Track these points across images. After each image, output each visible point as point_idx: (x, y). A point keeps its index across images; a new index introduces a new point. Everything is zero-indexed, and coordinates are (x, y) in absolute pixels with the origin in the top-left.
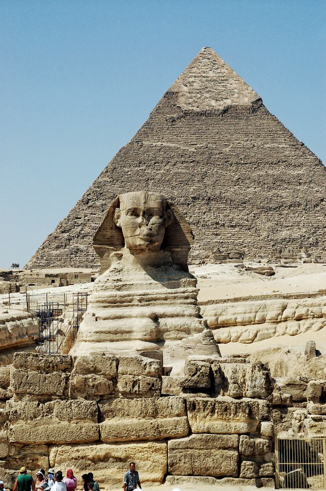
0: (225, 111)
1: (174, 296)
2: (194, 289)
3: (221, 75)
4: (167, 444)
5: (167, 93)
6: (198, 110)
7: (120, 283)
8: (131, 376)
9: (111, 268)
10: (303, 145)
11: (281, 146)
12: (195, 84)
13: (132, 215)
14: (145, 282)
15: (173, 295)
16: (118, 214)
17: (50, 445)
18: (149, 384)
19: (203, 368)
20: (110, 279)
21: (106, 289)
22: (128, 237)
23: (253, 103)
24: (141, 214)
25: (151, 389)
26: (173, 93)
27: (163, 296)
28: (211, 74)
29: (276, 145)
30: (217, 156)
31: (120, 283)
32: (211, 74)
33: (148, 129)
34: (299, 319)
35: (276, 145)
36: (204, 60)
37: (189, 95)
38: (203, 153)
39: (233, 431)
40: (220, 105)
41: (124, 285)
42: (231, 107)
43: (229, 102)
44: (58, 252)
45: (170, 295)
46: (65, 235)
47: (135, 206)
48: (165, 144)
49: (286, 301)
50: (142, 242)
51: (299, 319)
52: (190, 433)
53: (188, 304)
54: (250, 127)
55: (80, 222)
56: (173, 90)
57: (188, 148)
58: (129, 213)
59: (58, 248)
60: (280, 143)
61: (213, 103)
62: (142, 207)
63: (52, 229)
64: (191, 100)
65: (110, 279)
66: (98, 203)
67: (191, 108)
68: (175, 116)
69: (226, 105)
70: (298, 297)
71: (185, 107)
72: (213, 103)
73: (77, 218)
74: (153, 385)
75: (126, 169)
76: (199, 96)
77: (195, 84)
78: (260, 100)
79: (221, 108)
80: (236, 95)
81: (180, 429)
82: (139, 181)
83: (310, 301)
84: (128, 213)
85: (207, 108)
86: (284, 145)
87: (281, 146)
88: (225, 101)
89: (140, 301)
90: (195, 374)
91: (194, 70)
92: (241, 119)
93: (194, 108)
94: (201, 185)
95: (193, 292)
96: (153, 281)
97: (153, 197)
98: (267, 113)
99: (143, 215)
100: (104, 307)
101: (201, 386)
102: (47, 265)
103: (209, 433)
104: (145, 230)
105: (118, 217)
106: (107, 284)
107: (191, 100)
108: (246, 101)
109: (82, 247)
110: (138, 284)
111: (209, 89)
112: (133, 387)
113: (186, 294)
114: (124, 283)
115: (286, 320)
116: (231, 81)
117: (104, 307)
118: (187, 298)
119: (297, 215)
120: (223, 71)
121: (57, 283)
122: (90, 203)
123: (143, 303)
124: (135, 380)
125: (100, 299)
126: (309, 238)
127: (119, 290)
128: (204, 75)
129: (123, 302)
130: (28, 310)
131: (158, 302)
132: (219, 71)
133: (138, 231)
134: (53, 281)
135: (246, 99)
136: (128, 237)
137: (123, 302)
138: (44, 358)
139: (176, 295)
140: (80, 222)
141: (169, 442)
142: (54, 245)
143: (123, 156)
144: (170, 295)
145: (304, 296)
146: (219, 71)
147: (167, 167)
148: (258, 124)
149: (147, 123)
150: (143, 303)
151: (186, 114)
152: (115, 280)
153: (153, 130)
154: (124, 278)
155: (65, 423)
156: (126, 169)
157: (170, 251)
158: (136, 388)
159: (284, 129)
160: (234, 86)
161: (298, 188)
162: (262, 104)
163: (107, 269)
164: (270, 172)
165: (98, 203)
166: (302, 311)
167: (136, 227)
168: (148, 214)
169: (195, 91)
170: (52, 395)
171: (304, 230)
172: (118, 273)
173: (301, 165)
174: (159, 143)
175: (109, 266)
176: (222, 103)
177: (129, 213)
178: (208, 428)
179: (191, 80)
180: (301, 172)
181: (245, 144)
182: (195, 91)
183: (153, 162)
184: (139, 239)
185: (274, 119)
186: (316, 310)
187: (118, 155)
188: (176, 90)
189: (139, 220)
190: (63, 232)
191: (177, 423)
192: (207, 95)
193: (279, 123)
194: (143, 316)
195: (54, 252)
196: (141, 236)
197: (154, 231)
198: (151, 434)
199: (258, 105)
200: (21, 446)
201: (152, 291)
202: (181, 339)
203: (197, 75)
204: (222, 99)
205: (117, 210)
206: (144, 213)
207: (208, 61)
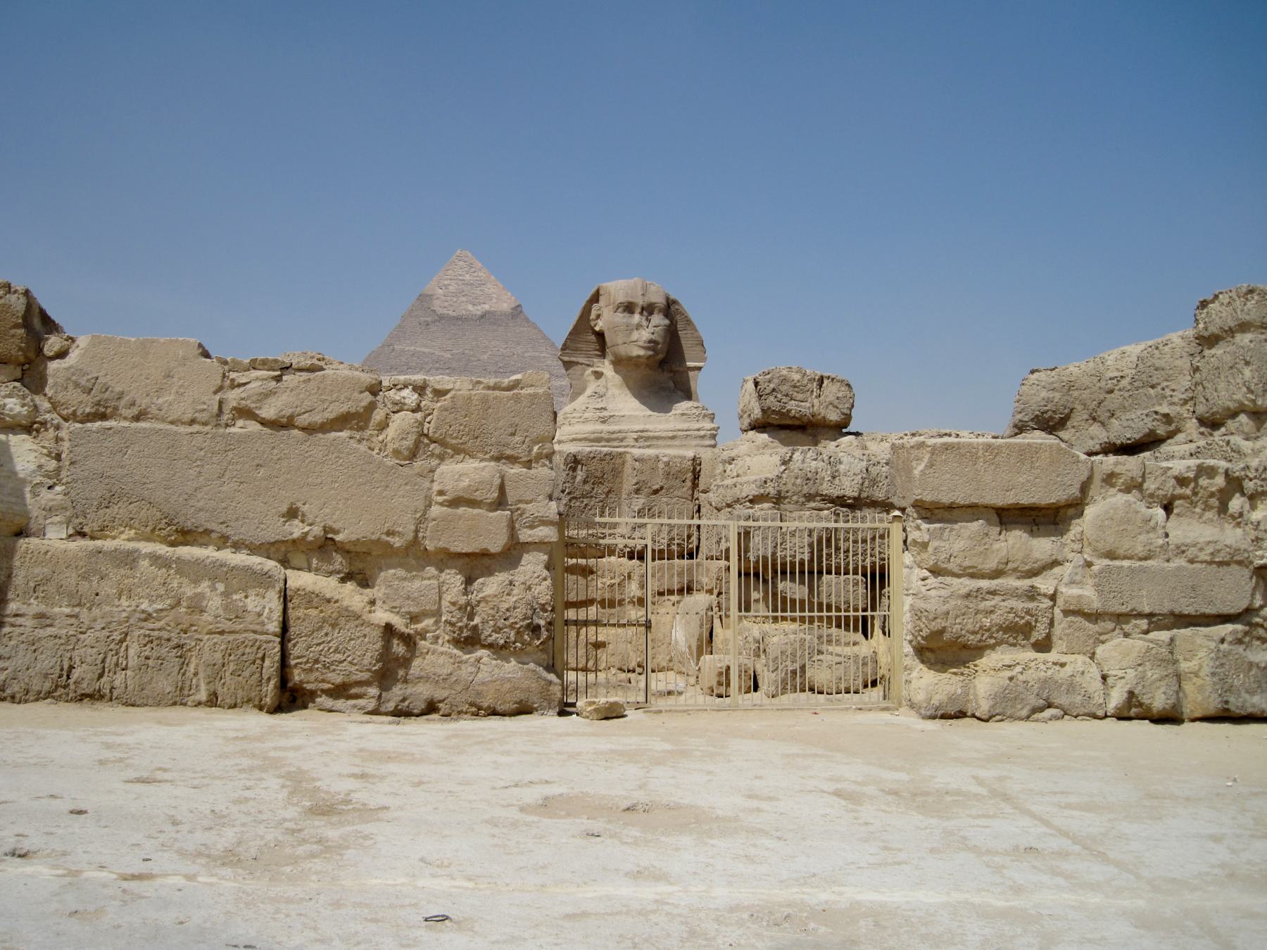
0: (483, 316)
1: (687, 436)
2: (712, 425)
3: (478, 278)
5: (420, 296)
6: (454, 314)
9: (589, 392)
12: (451, 287)
13: (624, 311)
14: (642, 414)
15: (684, 433)
16: (599, 312)
20: (591, 406)
21: (586, 421)
22: (618, 345)
23: (512, 309)
24: (639, 310)
26: (427, 296)
27: (671, 434)
28: (468, 277)
30: (475, 363)
32: (468, 277)
36: (460, 263)
37: (443, 298)
40: (477, 310)
41: (611, 416)
43: (487, 307)
45: (680, 433)
47: (631, 300)
48: (418, 349)
50: (642, 352)
53: (706, 446)
54: (509, 334)
56: (427, 293)
57: (442, 354)
58: (620, 310)
60: (541, 352)
61: (470, 307)
62: (640, 301)
64: (446, 304)
65: (591, 406)
67: (445, 311)
68: (429, 319)
69: (484, 310)
71: (440, 311)
72: (470, 307)
76: (455, 299)
77: (451, 287)
78: (519, 306)
79: (479, 313)
80: (494, 300)
84: (617, 309)
89: (636, 440)
91: (450, 272)
92: (500, 325)
93: (451, 313)
95: (710, 430)
96: (652, 413)
97: (652, 287)
98: (527, 320)
99: (641, 313)
104: (645, 335)
105: (598, 316)
106: (586, 415)
107: (446, 304)
108: (505, 306)
110: (631, 416)
111: (466, 293)
113: (702, 433)
114: (612, 414)
116: (489, 285)
117: (647, 431)
118: (703, 437)
120: (480, 274)
123: (641, 444)
125: (579, 436)
127: (604, 422)
128: (460, 278)
129: (614, 440)
131: (660, 442)
132: (476, 274)
133: (635, 336)
135: (505, 305)
136: (618, 345)
137: (614, 440)
139: (688, 433)
144: (680, 433)
146: (476, 274)
148: (518, 331)
149: (400, 326)
152: (598, 409)
154: (610, 407)
157: (671, 371)
159: (546, 338)
160: (492, 290)
162: (521, 312)
163: (580, 394)
167: (633, 330)
168: (649, 310)
169: (450, 294)
172: (600, 400)
174: (412, 348)
175: (584, 390)
176: (479, 308)
177: (620, 310)
179: (448, 282)
180: (564, 383)
181: (504, 351)
182: (450, 294)
183: (405, 367)
184: (636, 348)
185: (536, 327)
188: (430, 293)
189: (637, 318)
192: (464, 299)
193: (540, 331)
196: (641, 344)
199: (517, 311)
201: (656, 426)
203: (452, 278)
204: (480, 303)
205: (595, 307)
206: (643, 309)
207: (464, 263)
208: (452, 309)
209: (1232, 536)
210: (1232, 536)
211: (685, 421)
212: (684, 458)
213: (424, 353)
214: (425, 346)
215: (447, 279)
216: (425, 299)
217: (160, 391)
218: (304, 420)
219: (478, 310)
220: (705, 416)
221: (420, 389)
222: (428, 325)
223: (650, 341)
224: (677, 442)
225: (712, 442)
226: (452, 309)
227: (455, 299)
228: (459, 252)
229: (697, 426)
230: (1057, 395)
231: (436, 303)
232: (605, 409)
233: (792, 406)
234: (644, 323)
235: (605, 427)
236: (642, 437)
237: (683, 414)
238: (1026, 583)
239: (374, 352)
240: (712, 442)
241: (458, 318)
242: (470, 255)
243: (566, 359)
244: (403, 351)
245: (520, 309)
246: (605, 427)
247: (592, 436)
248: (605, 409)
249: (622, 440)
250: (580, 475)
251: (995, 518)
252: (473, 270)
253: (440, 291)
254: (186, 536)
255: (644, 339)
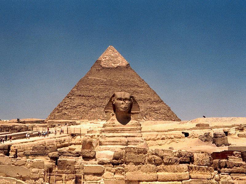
0: (117, 68)
2: (140, 127)
4: (182, 182)
5: (97, 61)
6: (108, 67)
7: (114, 124)
8: (169, 157)
9: (111, 119)
10: (143, 80)
11: (136, 80)
12: (107, 58)
17: (139, 181)
18: (175, 160)
19: (188, 155)
20: (111, 123)
21: (110, 126)
25: (176, 162)
26: (99, 61)
27: (129, 129)
29: (134, 80)
31: (114, 124)
32: (112, 55)
33: (90, 73)
34: (163, 139)
35: (134, 80)
37: (104, 61)
38: (109, 82)
39: (206, 178)
42: (119, 66)
43: (118, 65)
44: (58, 114)
46: (61, 108)
48: (96, 78)
49: (158, 133)
51: (163, 139)
52: (190, 178)
54: (125, 74)
55: (66, 104)
57: (104, 80)
59: (58, 113)
60: (136, 79)
61: (113, 65)
63: (56, 106)
64: (105, 63)
66: (72, 98)
68: (100, 68)
70: (161, 132)
71: (103, 66)
72: (113, 65)
73: (65, 102)
74: (177, 160)
75: (83, 86)
76: (108, 62)
78: (129, 64)
79: (116, 66)
80: (121, 62)
81: (187, 177)
82: (87, 91)
83: (166, 133)
85: (111, 66)
86: (136, 80)
87: (136, 80)
88: (117, 64)
90: (185, 157)
92: (122, 71)
93: (106, 66)
94: (108, 92)
97: (126, 94)
98: (131, 69)
100: (109, 133)
101: (187, 161)
102: (54, 119)
103: (197, 178)
105: (114, 101)
106: (110, 125)
107: (105, 63)
109: (66, 113)
112: (169, 160)
113: (137, 129)
115: (158, 139)
116: (119, 57)
119: (141, 104)
120: (116, 54)
121: (68, 125)
122: (70, 98)
124: (170, 158)
126: (145, 112)
127: (114, 126)
130: (68, 133)
132: (115, 54)
134: (66, 124)
135: (124, 64)
137: (116, 131)
138: (137, 149)
140: (66, 104)
141: (183, 181)
142: (57, 112)
143: (81, 81)
145: (164, 131)
147: (97, 86)
149: (90, 71)
150: (122, 132)
151: (103, 68)
153: (92, 73)
155: (145, 173)
156: (83, 86)
158: (170, 161)
160: (120, 59)
161: (141, 95)
162: (129, 66)
164: (132, 89)
165: (72, 98)
166: (164, 136)
170: (140, 163)
171: (143, 109)
173: (142, 87)
174: (94, 78)
176: (116, 65)
178: (197, 176)
179: (105, 56)
186: (169, 136)
187: (80, 81)
190: (60, 107)
191: (186, 174)
192: (111, 62)
194: (123, 136)
195: (57, 114)
196: (123, 108)
197: (126, 106)
198: (176, 178)
199: (128, 65)
200: (129, 181)
202: (136, 145)
208: (107, 65)
209: (122, 177)
210: (122, 177)
211: (134, 126)
212: (73, 161)
213: (98, 79)
214: (98, 77)
215: (106, 55)
216: (98, 62)
217: (5, 162)
218: (19, 165)
219: (115, 66)
220: (139, 125)
221: (31, 161)
222: (99, 70)
223: (125, 107)
224: (131, 131)
225: (140, 131)
226: (107, 65)
227: (108, 62)
228: (110, 46)
229: (136, 127)
230: (117, 155)
231: (102, 63)
232: (114, 123)
233: (87, 155)
234: (124, 103)
235: (114, 128)
236: (122, 130)
237: (133, 125)
238: (96, 181)
239: (82, 79)
240: (140, 131)
241: (109, 68)
242: (113, 47)
243: (106, 111)
244: (91, 79)
245: (129, 65)
246: (114, 128)
247: (110, 130)
248: (114, 123)
249: (118, 131)
250: (60, 163)
251: (93, 175)
252: (114, 52)
253: (103, 59)
254: (7, 176)
255: (123, 107)
